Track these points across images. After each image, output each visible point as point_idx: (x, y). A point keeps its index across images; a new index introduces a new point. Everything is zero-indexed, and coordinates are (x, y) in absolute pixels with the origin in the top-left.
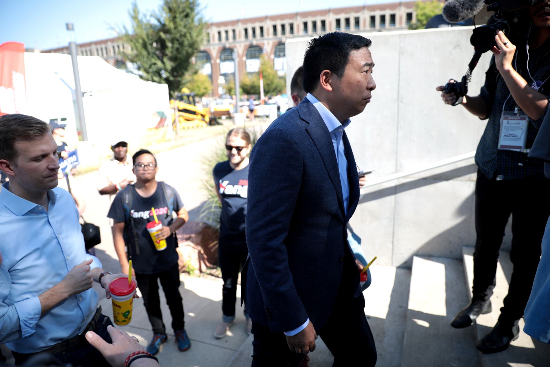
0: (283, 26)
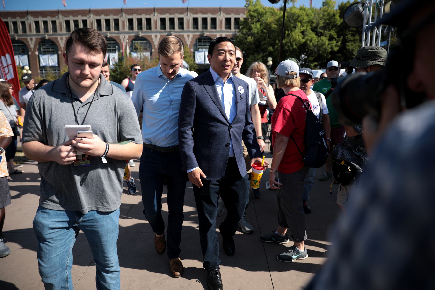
0: (108, 21)
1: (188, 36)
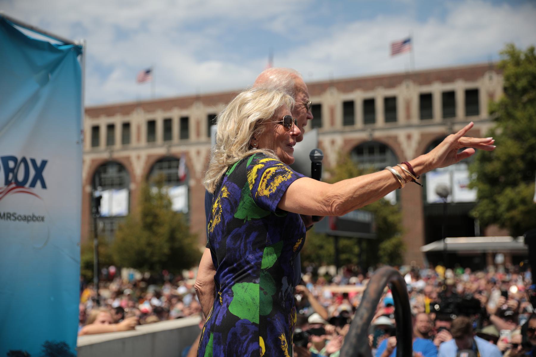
1: (409, 137)
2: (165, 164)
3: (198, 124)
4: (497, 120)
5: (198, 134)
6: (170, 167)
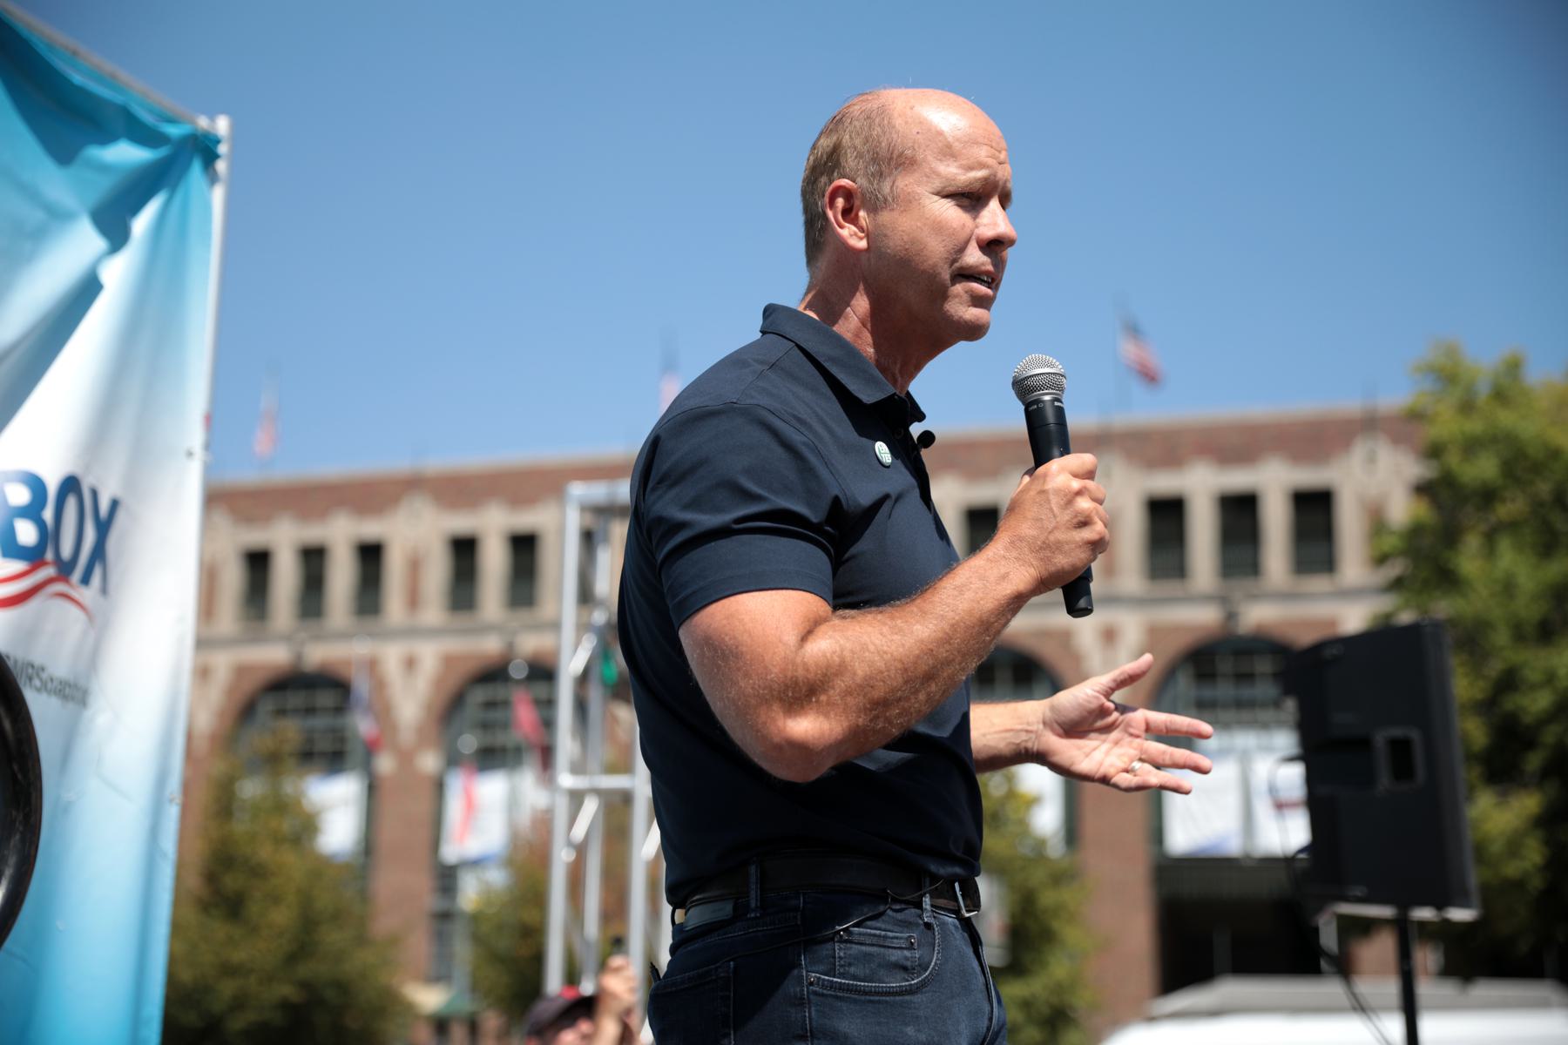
2: (295, 699)
3: (415, 566)
4: (1397, 585)
5: (414, 600)
6: (310, 711)
